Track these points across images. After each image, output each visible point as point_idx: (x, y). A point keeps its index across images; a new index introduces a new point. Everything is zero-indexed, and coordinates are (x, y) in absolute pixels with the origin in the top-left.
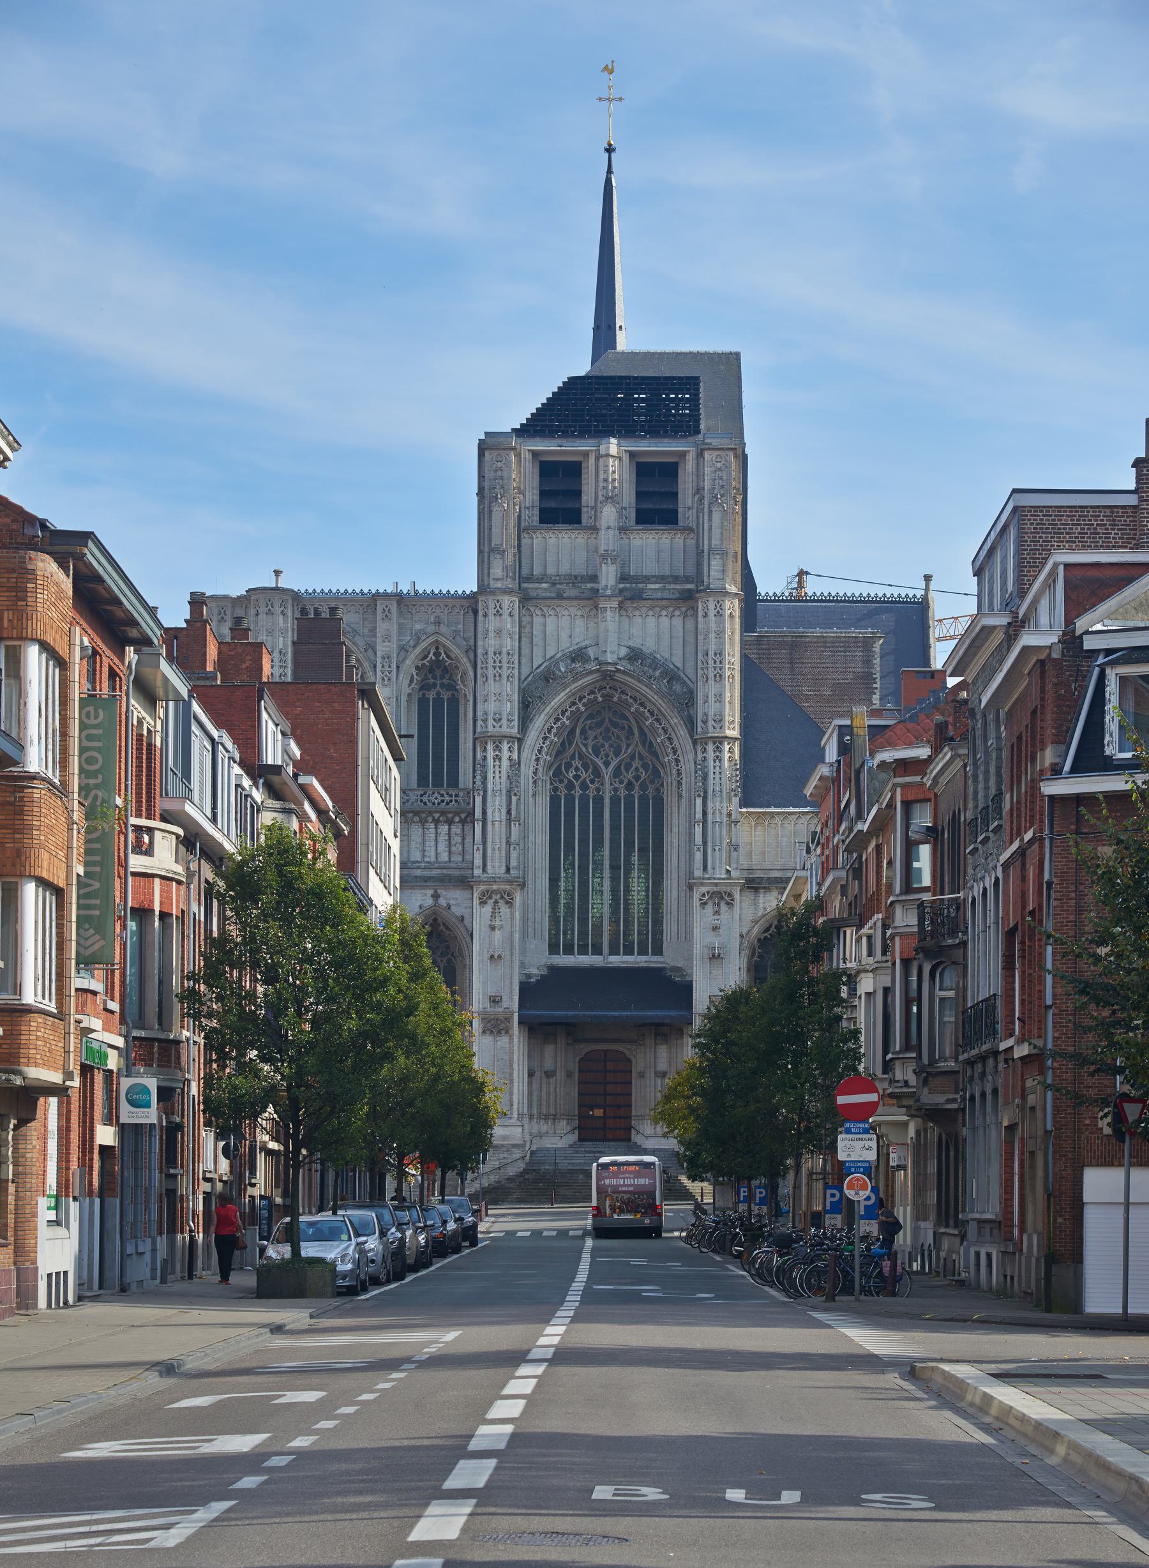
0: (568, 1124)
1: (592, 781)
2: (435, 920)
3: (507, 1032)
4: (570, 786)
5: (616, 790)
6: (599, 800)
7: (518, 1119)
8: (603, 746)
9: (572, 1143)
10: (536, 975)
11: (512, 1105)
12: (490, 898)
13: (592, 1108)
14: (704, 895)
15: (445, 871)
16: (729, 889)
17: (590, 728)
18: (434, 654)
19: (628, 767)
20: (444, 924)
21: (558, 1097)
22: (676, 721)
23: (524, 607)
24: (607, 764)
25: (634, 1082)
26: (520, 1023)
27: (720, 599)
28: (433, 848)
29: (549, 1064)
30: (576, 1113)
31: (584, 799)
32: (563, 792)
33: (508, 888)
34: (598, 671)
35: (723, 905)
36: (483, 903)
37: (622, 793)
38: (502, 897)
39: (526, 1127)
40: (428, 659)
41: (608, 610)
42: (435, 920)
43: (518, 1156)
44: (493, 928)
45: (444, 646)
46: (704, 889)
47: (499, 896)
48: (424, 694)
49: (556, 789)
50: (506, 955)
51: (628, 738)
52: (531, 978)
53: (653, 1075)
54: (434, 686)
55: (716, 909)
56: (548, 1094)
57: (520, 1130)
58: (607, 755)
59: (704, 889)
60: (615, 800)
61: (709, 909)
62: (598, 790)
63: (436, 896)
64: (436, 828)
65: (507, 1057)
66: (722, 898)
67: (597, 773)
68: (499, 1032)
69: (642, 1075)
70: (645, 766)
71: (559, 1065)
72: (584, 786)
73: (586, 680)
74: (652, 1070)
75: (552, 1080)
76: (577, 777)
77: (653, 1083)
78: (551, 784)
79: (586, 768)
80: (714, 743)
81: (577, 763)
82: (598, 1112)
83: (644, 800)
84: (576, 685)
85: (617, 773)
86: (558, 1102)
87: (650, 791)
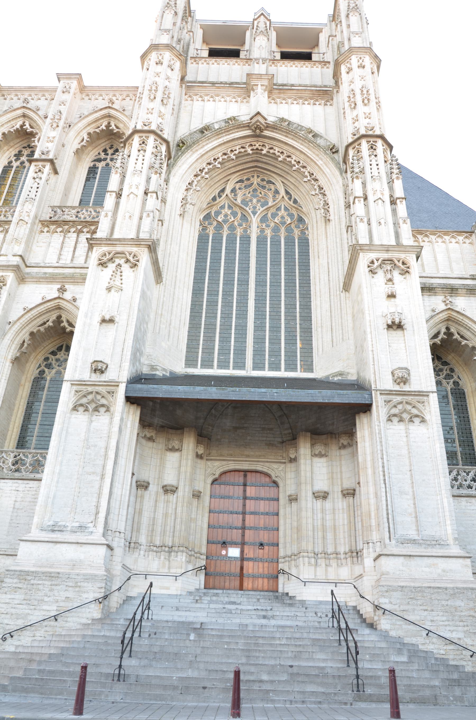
0: (189, 562)
1: (240, 225)
2: (59, 317)
3: (108, 410)
4: (220, 226)
5: (262, 231)
6: (246, 239)
7: (104, 535)
8: (251, 201)
9: (192, 589)
10: (164, 370)
11: (97, 513)
12: (111, 260)
13: (224, 544)
14: (372, 262)
15: (78, 270)
16: (402, 256)
17: (240, 189)
18: (106, 126)
19: (274, 215)
20: (68, 321)
21: (178, 520)
22: (321, 162)
23: (186, 94)
24: (254, 213)
25: (281, 512)
26: (130, 400)
27: (362, 56)
28: (71, 254)
29: (170, 479)
30: (204, 550)
31: (231, 240)
32: (211, 231)
33: (134, 249)
34: (248, 126)
35: (396, 274)
36: (102, 264)
37: (269, 233)
38: (127, 261)
39: (118, 551)
40: (100, 129)
41: (259, 86)
42: (59, 317)
43: (91, 596)
44: (109, 289)
45: (115, 118)
46: (373, 256)
47: (122, 261)
48: (94, 165)
49: (205, 229)
50: (121, 319)
51: (274, 196)
52: (156, 370)
53: (310, 494)
54: (105, 159)
55: (389, 276)
56: (166, 515)
57: (103, 550)
58: (255, 208)
59: (373, 256)
60: (261, 241)
61: (380, 277)
62: (245, 230)
63: (62, 290)
64: (78, 236)
65: (102, 444)
66: (395, 266)
67: (244, 218)
68: (96, 410)
69: (293, 499)
70: (291, 216)
71: (182, 476)
72: (232, 228)
73: (237, 134)
74: (309, 487)
75: (172, 498)
76: (225, 221)
77: (310, 505)
78: (201, 224)
79: (234, 214)
80: (368, 142)
81: (226, 210)
82: (234, 552)
83: (290, 241)
84: (228, 137)
85: (264, 219)
86: (178, 527)
87: (297, 233)
